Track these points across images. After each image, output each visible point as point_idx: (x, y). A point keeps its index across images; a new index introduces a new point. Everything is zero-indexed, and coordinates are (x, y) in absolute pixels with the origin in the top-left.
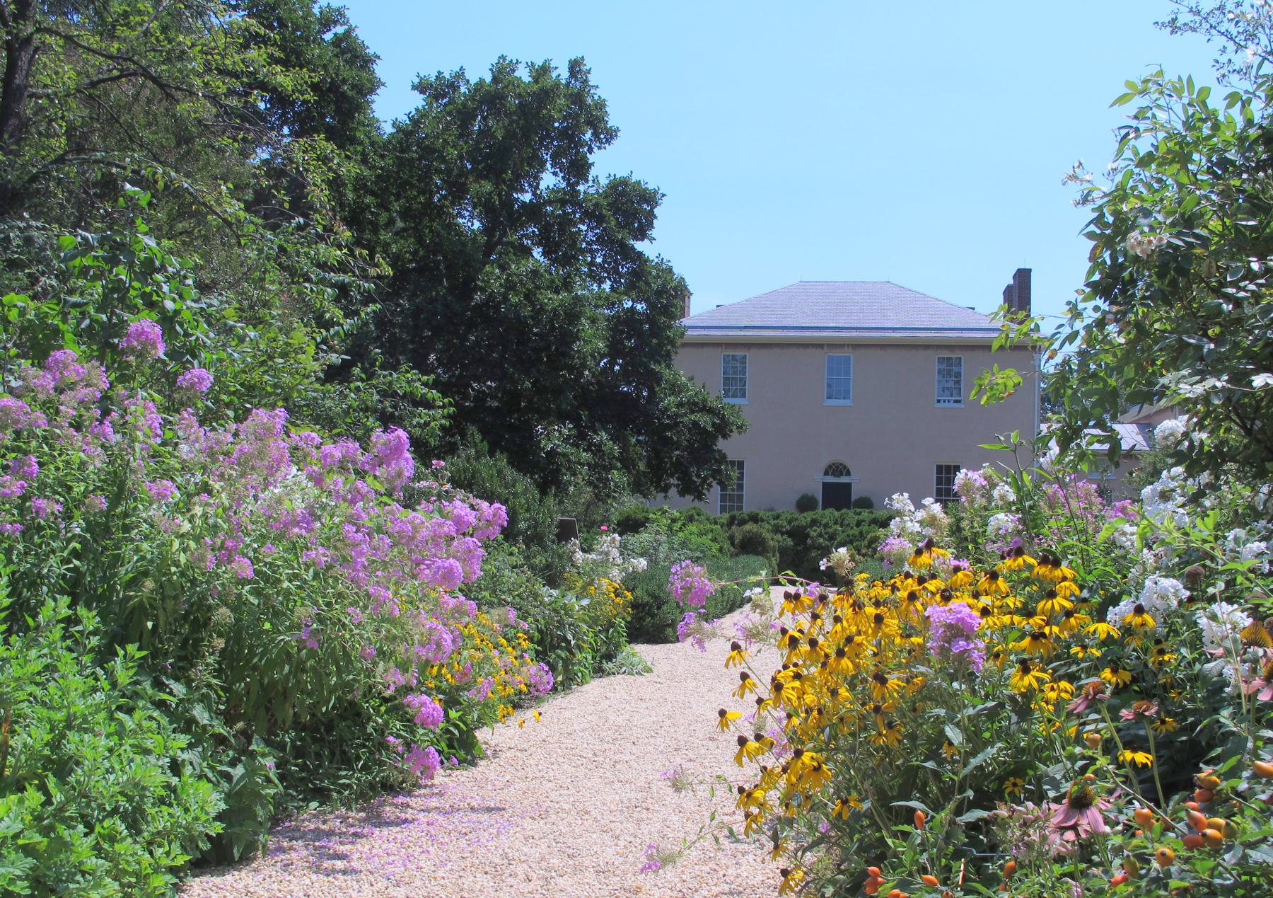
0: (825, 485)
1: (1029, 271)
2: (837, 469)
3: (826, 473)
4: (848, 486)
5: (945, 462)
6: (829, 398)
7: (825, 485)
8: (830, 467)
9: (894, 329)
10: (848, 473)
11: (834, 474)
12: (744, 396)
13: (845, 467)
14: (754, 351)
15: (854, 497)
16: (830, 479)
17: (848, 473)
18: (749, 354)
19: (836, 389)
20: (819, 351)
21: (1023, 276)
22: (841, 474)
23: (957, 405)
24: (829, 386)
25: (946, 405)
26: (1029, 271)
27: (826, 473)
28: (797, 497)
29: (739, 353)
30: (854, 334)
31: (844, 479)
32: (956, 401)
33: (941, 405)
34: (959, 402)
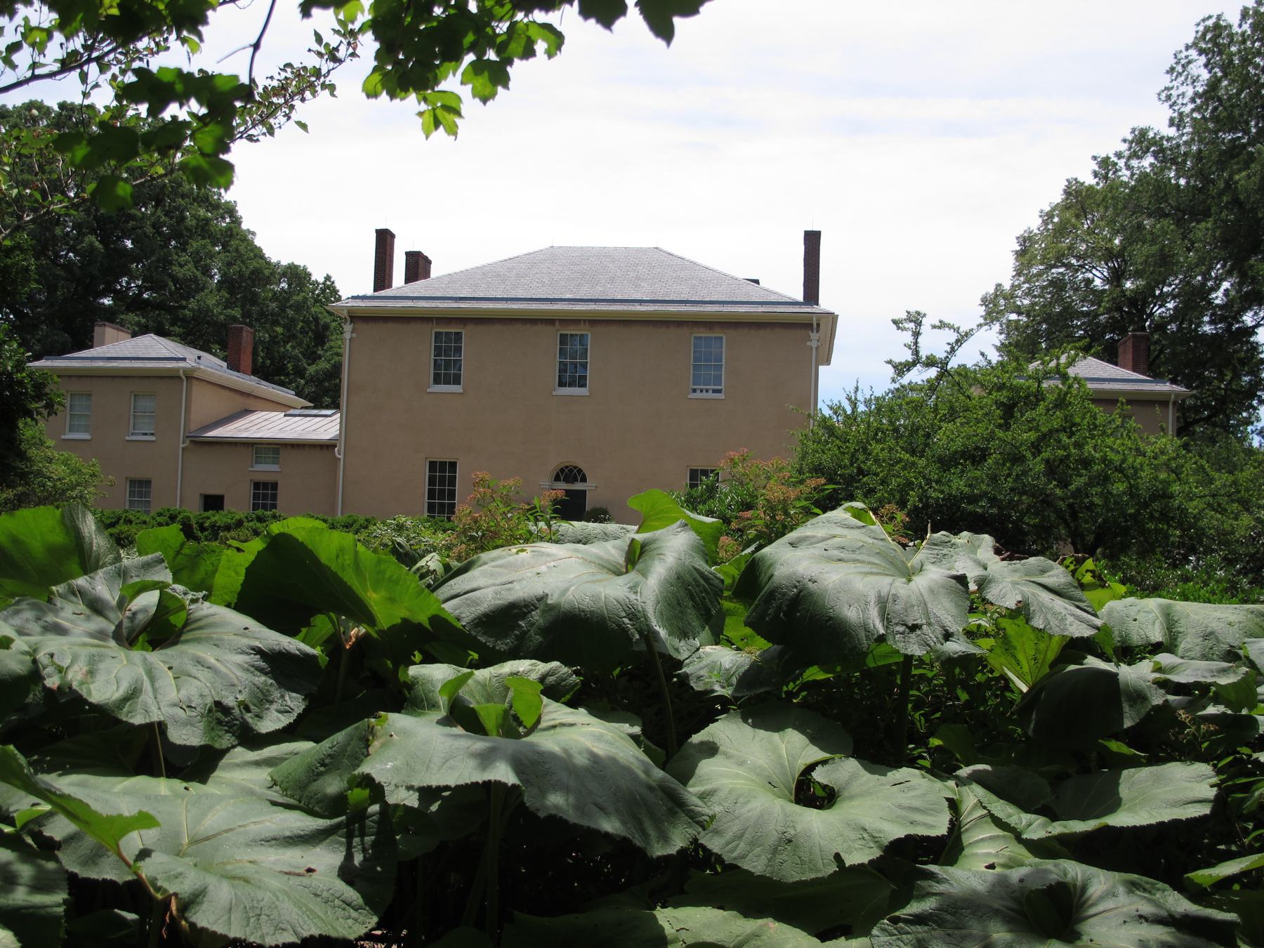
3: (557, 478)
6: (561, 384)
8: (562, 470)
9: (641, 302)
10: (584, 479)
11: (567, 480)
12: (457, 380)
13: (580, 471)
14: (470, 327)
17: (584, 479)
18: (465, 332)
19: (572, 375)
20: (548, 329)
21: (812, 240)
22: (575, 480)
25: (704, 395)
27: (557, 478)
29: (453, 329)
30: (592, 307)
31: (578, 486)
32: (715, 391)
33: (698, 395)
34: (719, 391)
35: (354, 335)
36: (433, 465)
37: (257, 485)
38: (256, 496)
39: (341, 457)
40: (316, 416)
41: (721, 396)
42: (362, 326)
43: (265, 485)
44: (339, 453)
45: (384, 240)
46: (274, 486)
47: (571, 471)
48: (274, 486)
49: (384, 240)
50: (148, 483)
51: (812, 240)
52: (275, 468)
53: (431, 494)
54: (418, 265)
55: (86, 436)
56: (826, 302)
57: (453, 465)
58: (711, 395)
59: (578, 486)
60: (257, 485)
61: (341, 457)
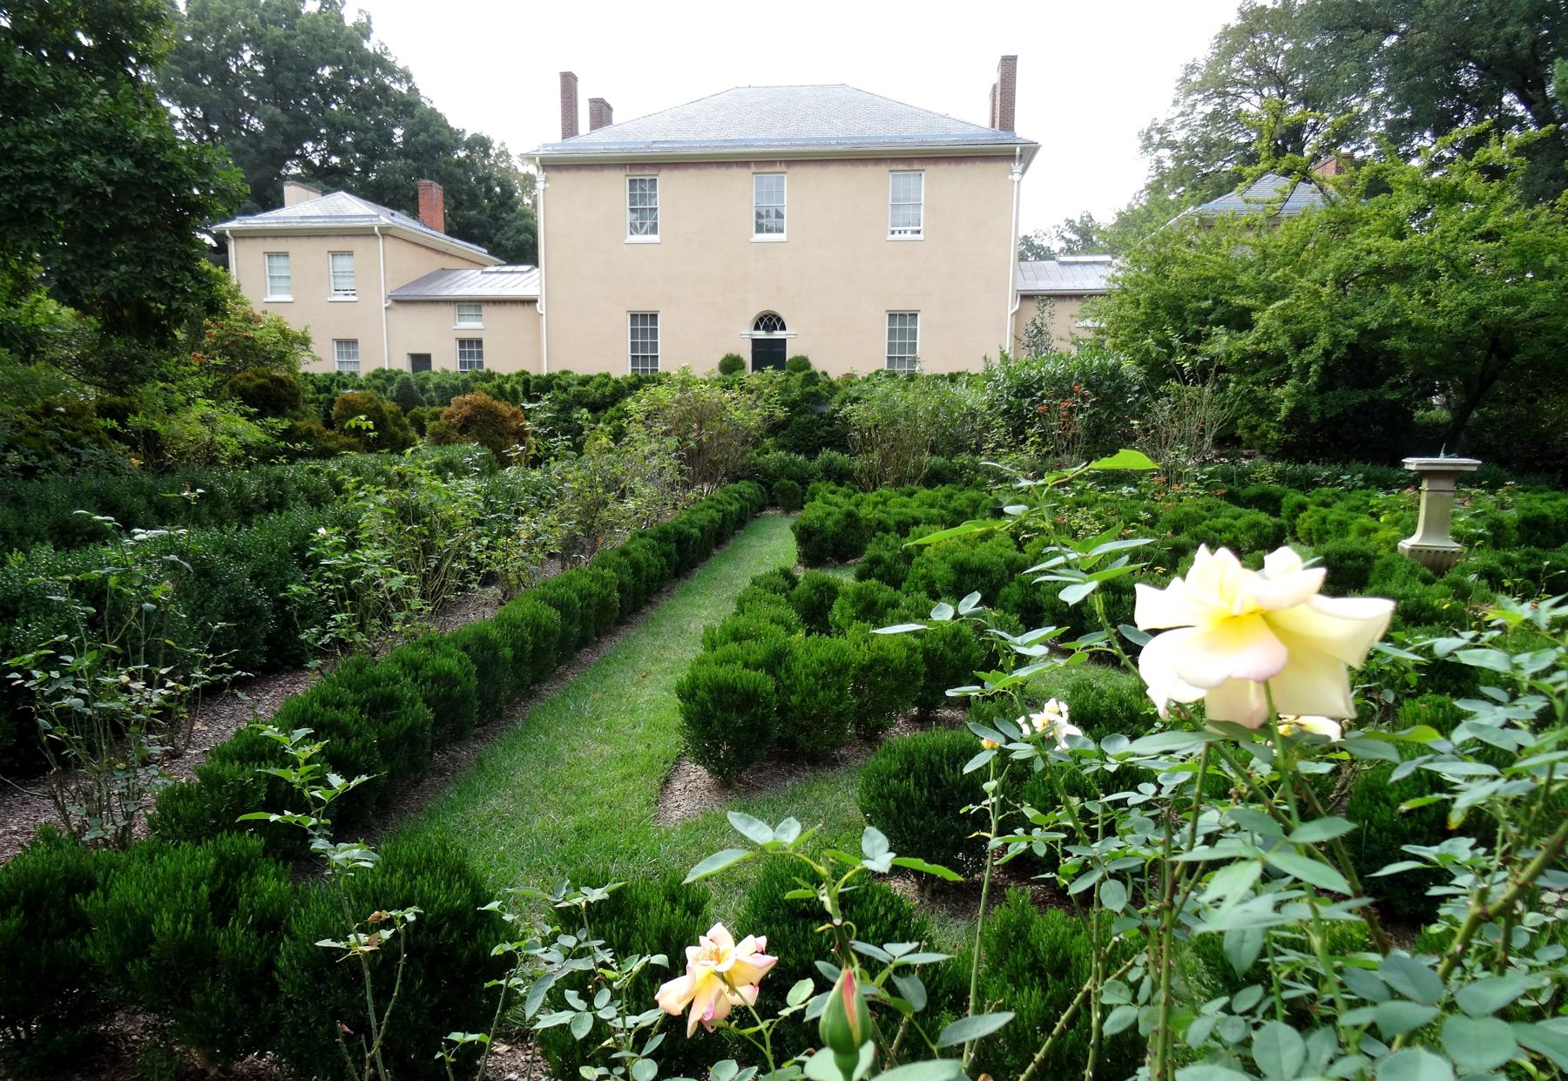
0: (756, 342)
1: (1014, 58)
2: (769, 321)
3: (757, 328)
4: (783, 341)
5: (900, 306)
7: (756, 342)
8: (761, 319)
10: (783, 328)
11: (766, 328)
12: (654, 229)
13: (779, 319)
15: (788, 357)
16: (761, 334)
17: (783, 328)
21: (1009, 65)
23: (916, 236)
24: (759, 215)
26: (1014, 58)
27: (757, 328)
28: (718, 357)
31: (778, 335)
32: (914, 232)
33: (897, 236)
34: (919, 232)
35: (548, 185)
36: (634, 317)
37: (462, 342)
38: (462, 354)
39: (544, 312)
40: (512, 272)
41: (920, 237)
42: (558, 177)
43: (471, 342)
44: (541, 307)
45: (569, 82)
46: (479, 342)
47: (770, 319)
48: (479, 342)
49: (569, 82)
50: (355, 342)
51: (1009, 65)
52: (478, 325)
53: (634, 346)
54: (602, 113)
55: (288, 298)
56: (1024, 128)
57: (654, 317)
58: (909, 236)
59: (778, 335)
60: (462, 342)
61: (544, 312)
